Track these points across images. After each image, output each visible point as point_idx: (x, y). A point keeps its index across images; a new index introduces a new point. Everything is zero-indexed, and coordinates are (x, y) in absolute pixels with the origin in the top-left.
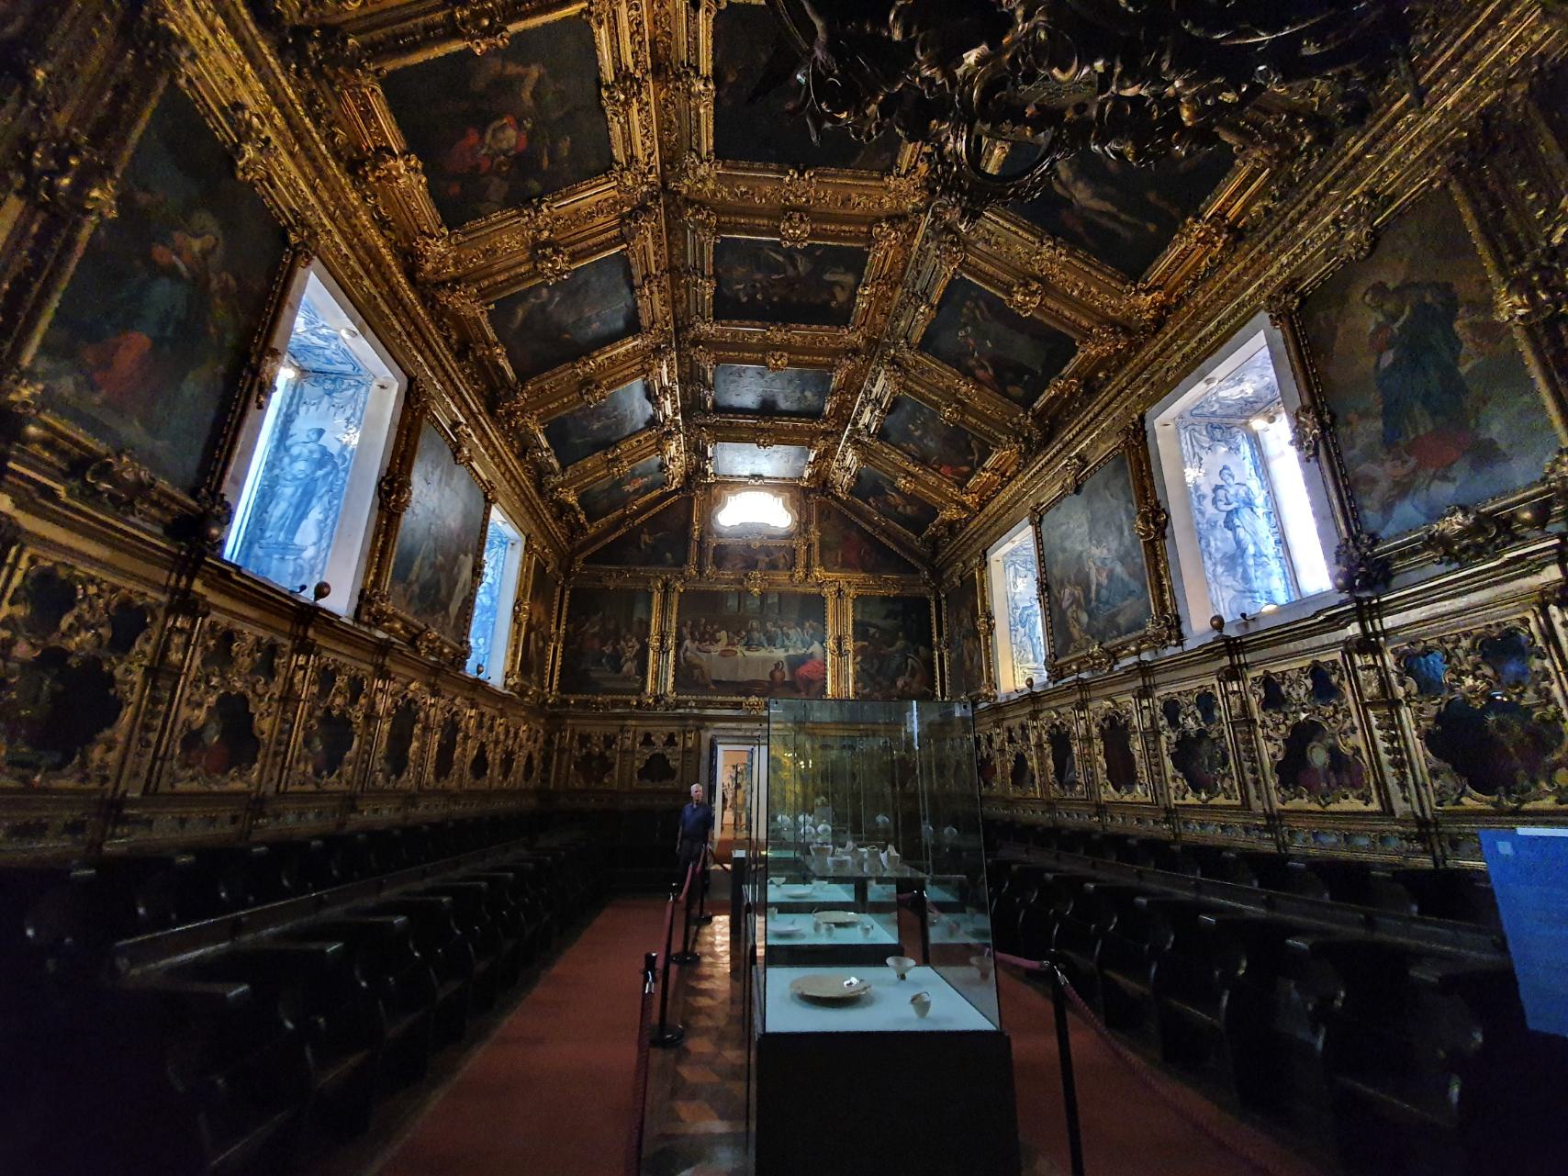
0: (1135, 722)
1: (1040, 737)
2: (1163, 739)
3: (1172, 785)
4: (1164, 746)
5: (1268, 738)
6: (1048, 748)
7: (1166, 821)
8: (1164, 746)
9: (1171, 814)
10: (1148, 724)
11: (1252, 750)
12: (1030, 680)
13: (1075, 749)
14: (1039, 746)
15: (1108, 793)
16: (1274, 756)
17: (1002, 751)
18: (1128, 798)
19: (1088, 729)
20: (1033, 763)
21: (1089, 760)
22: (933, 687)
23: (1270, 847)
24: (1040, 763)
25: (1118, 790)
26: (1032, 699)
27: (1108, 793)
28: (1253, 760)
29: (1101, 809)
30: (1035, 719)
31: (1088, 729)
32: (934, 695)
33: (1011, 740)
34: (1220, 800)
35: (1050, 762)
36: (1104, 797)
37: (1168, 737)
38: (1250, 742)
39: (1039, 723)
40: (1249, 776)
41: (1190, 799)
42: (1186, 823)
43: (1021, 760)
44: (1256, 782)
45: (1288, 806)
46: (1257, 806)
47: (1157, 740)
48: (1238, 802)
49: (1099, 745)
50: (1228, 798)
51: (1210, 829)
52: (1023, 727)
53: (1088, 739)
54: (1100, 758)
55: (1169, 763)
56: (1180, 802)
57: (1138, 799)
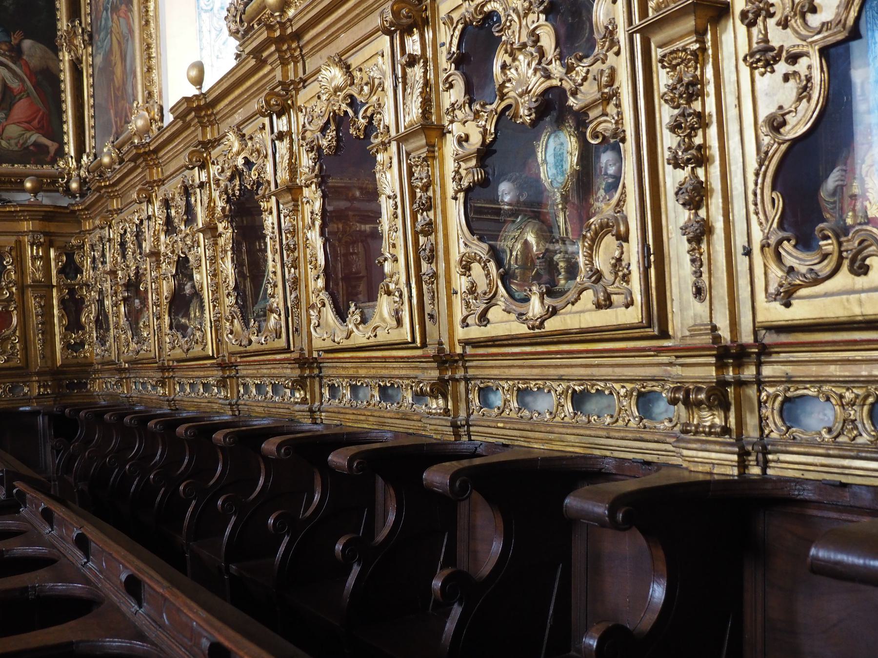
0: (388, 118)
1: (211, 209)
2: (450, 146)
3: (461, 283)
4: (450, 166)
5: (764, 57)
6: (226, 232)
7: (440, 389)
8: (450, 166)
9: (450, 367)
10: (413, 111)
11: (702, 120)
12: (200, 67)
13: (270, 221)
14: (211, 230)
15: (326, 329)
16: (776, 124)
17: (155, 254)
18: (360, 337)
19: (293, 169)
20: (202, 277)
21: (291, 249)
22: (58, 136)
23: (717, 462)
24: (216, 272)
25: (342, 314)
26: (199, 110)
27: (326, 329)
28: (701, 159)
29: (309, 367)
30: (203, 166)
31: (293, 169)
32: (61, 153)
33: (169, 226)
34: (581, 314)
35: (228, 267)
36: (320, 340)
37: (468, 130)
38: (692, 90)
39: (214, 170)
40: (677, 216)
41: (503, 323)
42: (484, 393)
43: (183, 267)
44: (700, 233)
45: (802, 310)
46: (686, 313)
47: (432, 154)
48: (633, 315)
49: (313, 200)
50: (606, 303)
51: (544, 404)
52: (187, 191)
53: (293, 190)
54: (315, 237)
55: (456, 212)
56: (476, 332)
57: (383, 337)
